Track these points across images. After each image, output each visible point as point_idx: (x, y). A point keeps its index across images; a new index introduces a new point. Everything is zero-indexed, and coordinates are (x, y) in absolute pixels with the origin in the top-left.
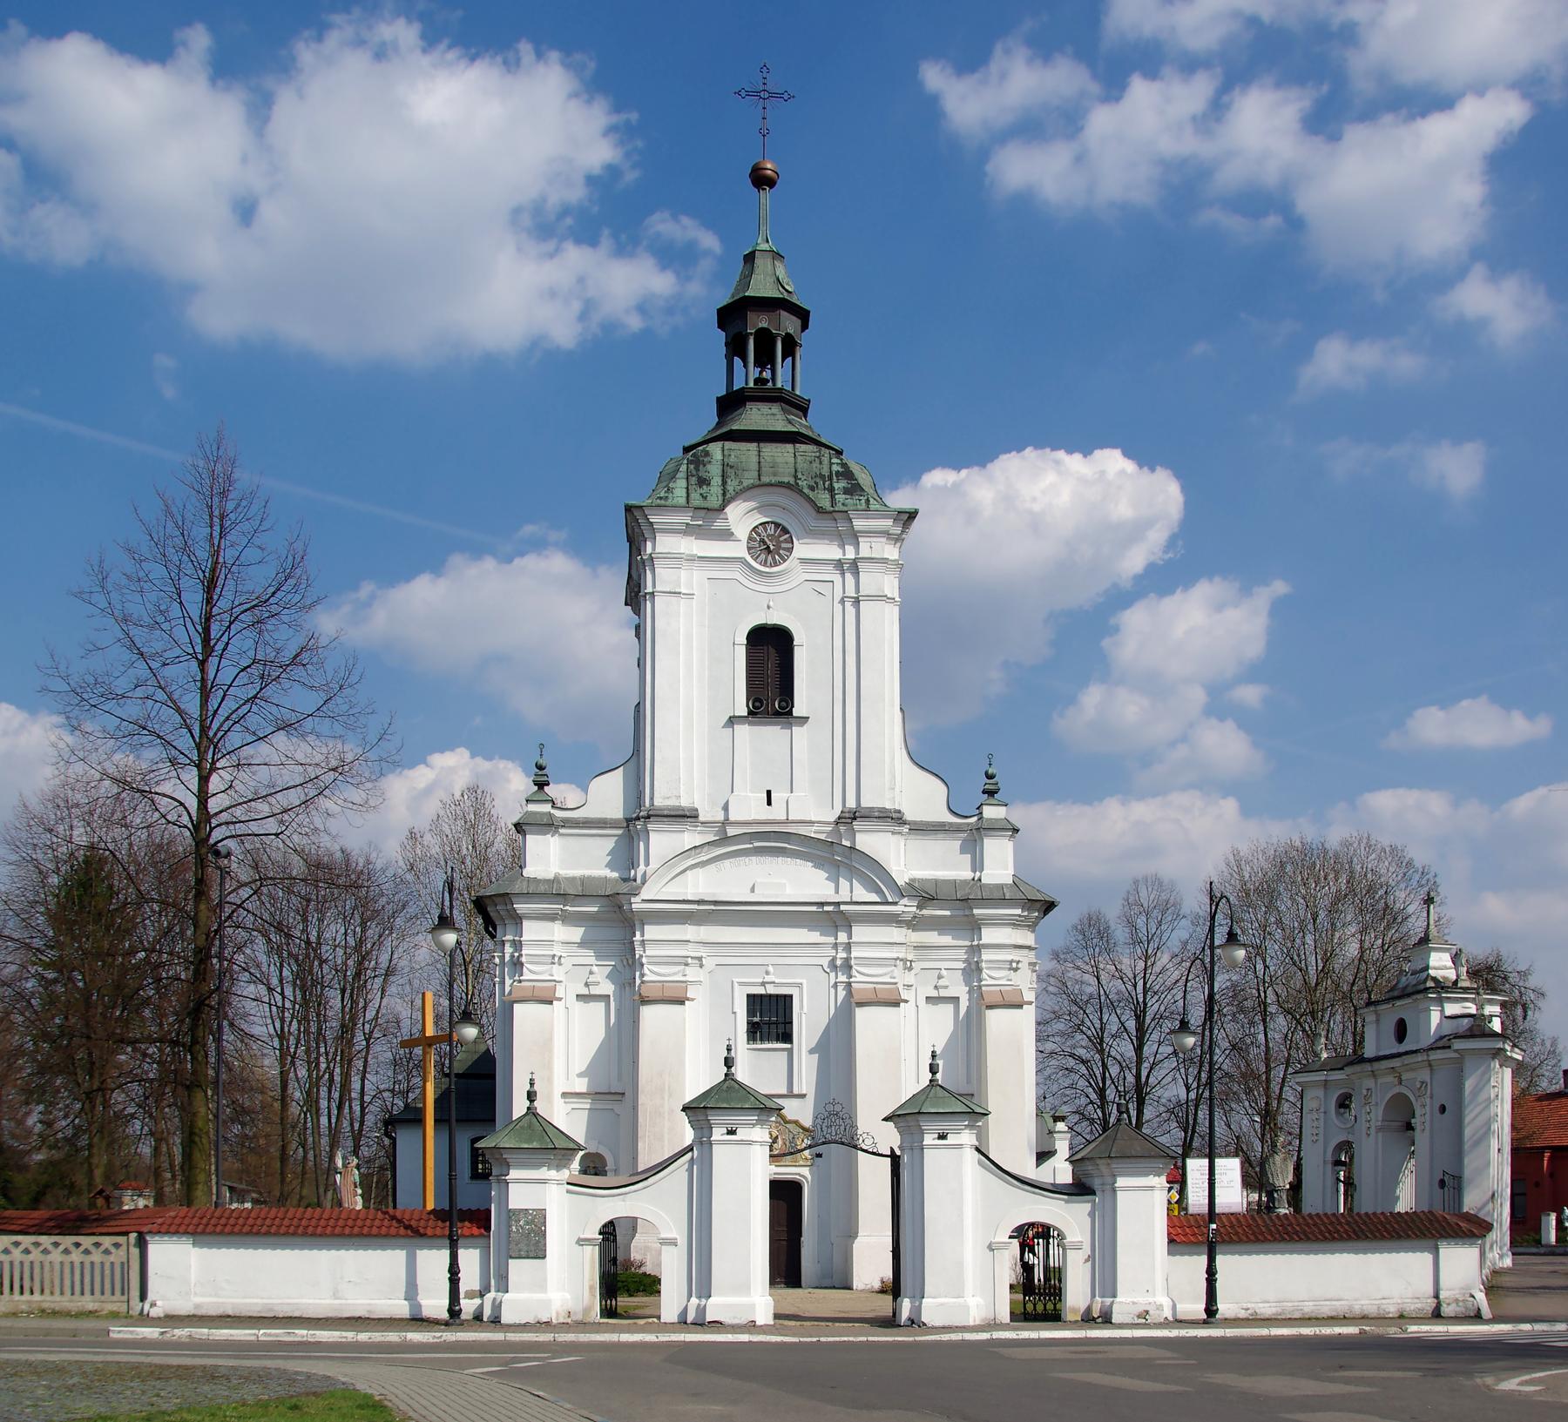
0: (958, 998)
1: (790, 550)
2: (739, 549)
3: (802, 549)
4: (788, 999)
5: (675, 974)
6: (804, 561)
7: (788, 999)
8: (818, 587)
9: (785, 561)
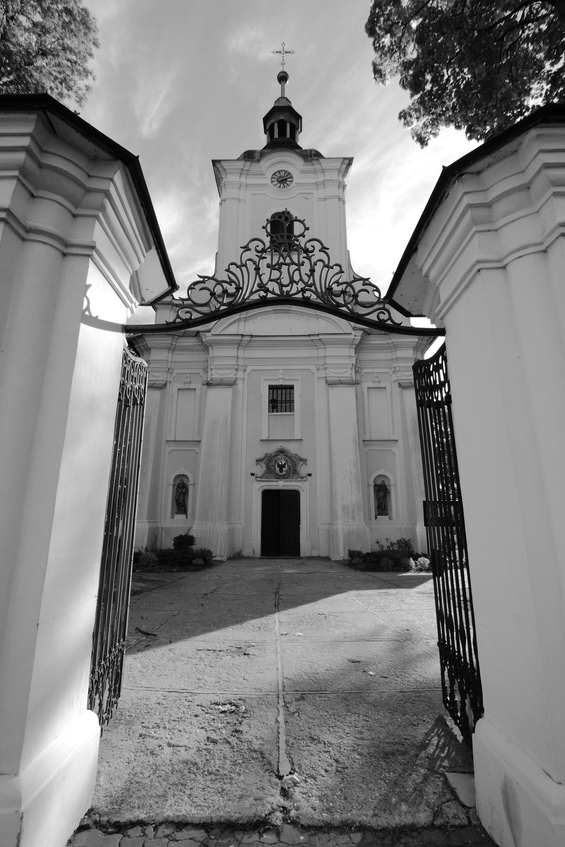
0: (385, 388)
1: (292, 182)
2: (269, 181)
3: (295, 180)
4: (291, 388)
5: (229, 374)
6: (298, 184)
7: (291, 388)
8: (306, 196)
9: (289, 186)
